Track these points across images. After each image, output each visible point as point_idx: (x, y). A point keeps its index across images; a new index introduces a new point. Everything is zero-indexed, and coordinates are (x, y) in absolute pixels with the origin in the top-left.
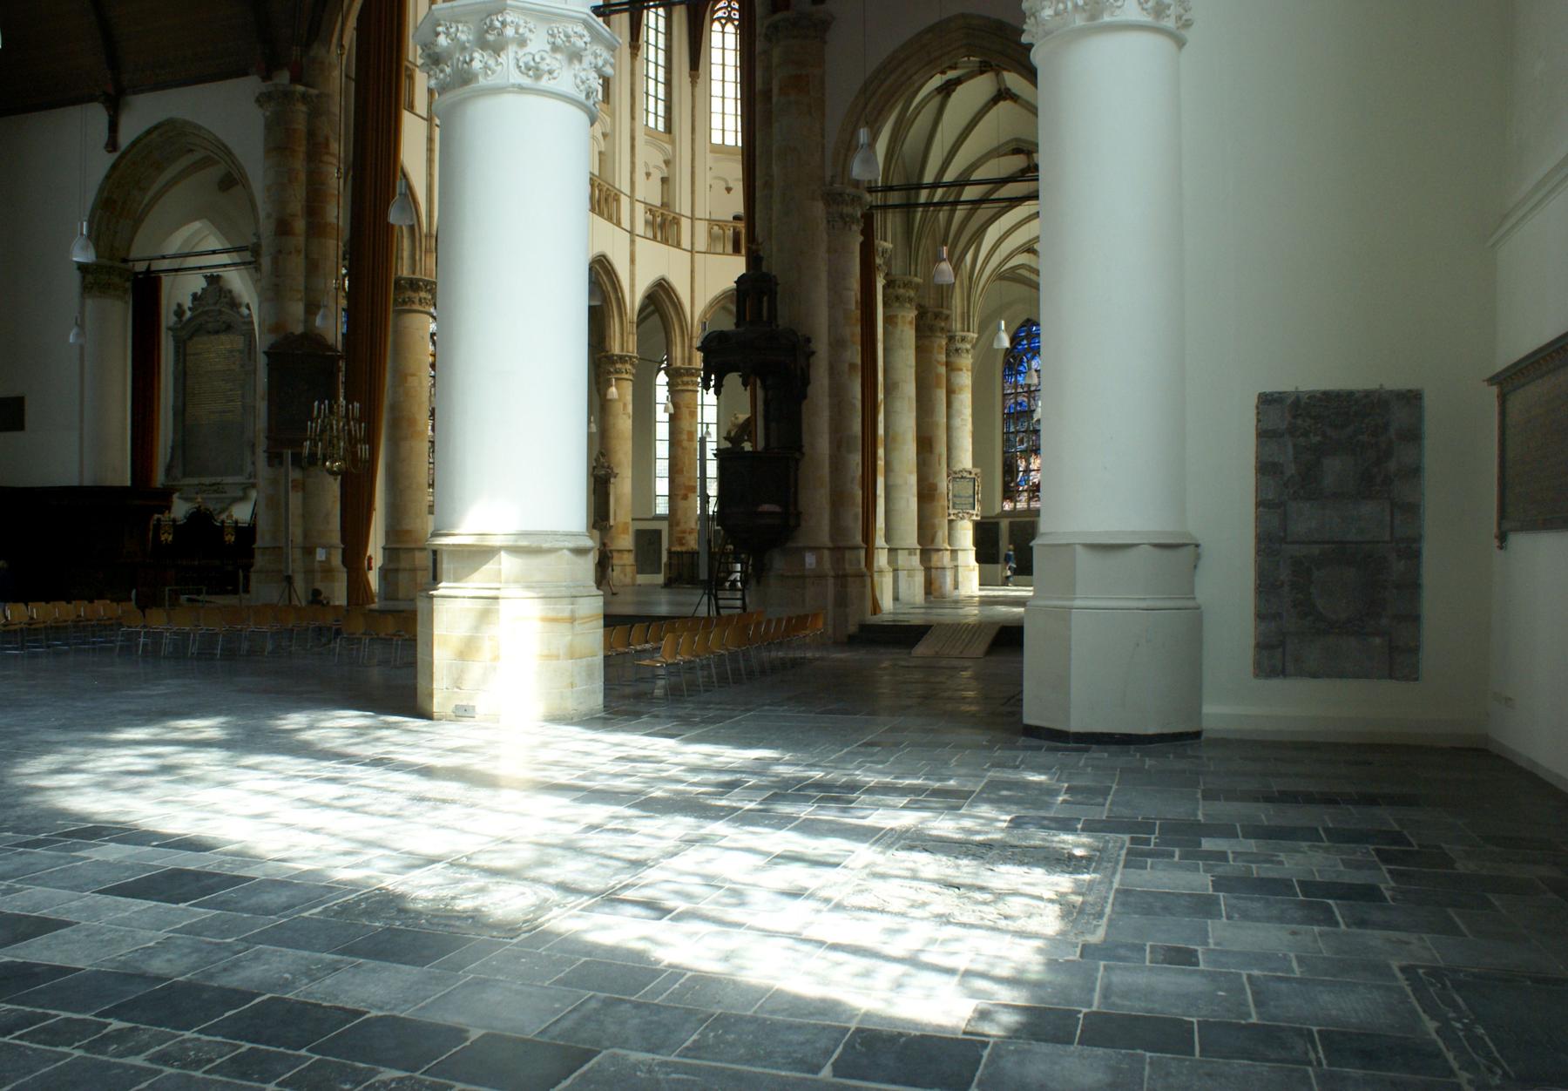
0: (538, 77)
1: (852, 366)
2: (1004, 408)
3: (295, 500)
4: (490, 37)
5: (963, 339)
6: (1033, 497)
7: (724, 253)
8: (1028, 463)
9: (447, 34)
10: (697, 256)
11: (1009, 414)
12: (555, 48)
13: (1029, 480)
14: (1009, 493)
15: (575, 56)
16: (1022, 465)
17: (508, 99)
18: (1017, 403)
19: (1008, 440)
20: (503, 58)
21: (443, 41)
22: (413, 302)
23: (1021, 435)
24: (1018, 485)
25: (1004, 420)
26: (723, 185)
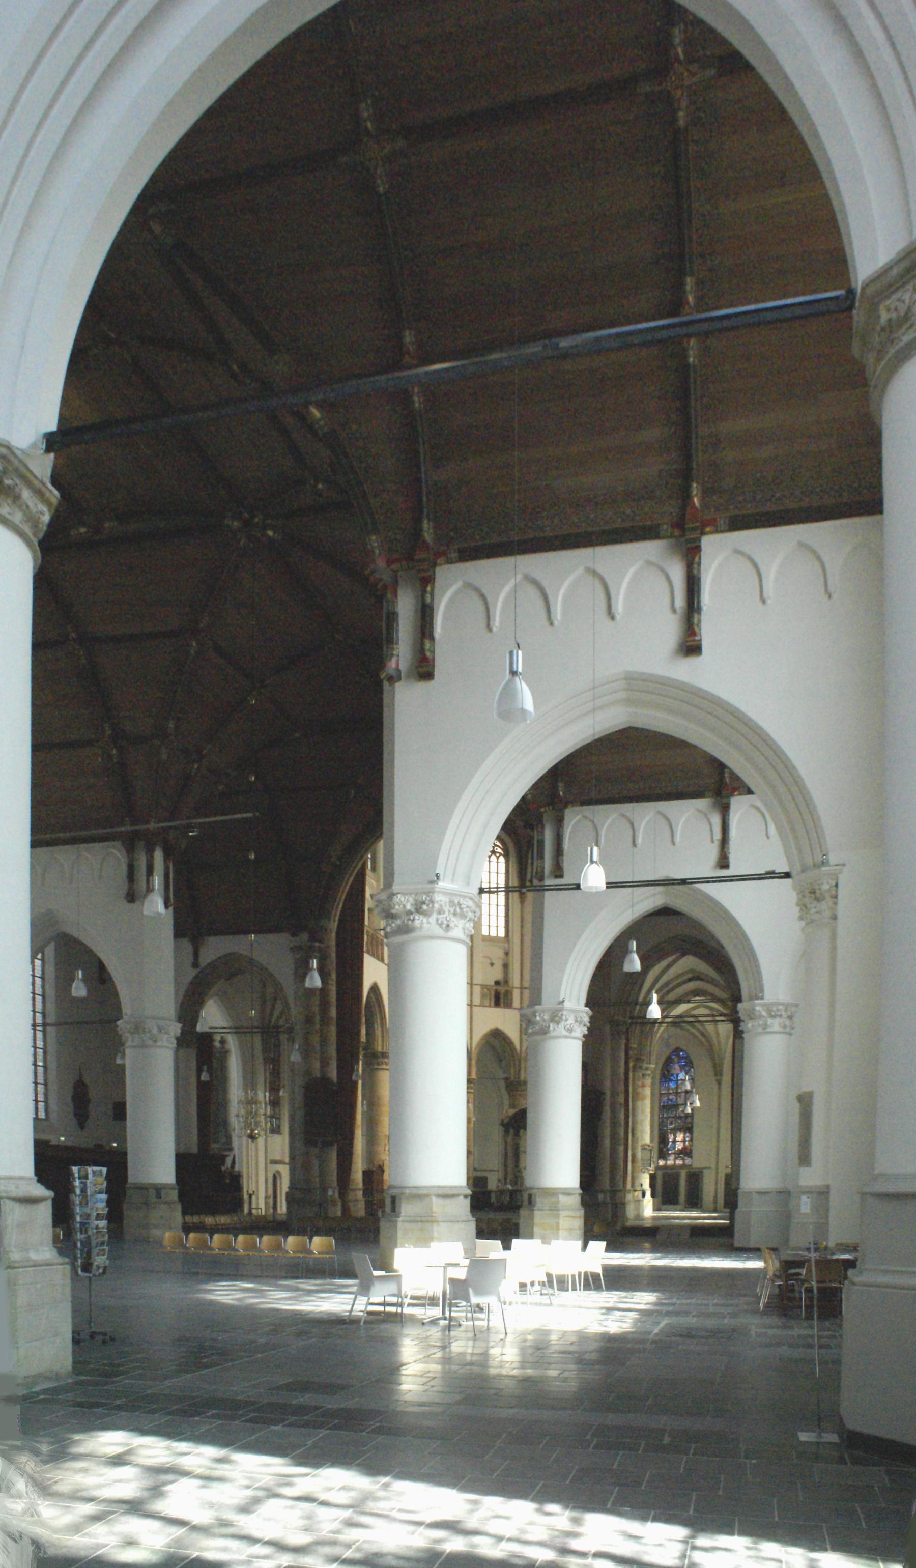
0: (571, 1032)
1: (621, 1104)
2: (660, 1103)
3: (316, 1163)
4: (557, 1019)
5: (647, 1069)
6: (678, 1157)
7: (490, 1006)
8: (675, 1136)
9: (540, 1016)
10: (474, 1008)
11: (664, 1106)
12: (576, 1021)
13: (675, 1147)
14: (663, 1155)
15: (580, 1023)
16: (671, 1138)
17: (562, 1040)
18: (668, 1099)
19: (663, 1122)
20: (560, 1026)
21: (538, 1018)
22: (382, 1064)
23: (670, 1119)
24: (668, 1150)
25: (660, 1109)
26: (489, 961)
